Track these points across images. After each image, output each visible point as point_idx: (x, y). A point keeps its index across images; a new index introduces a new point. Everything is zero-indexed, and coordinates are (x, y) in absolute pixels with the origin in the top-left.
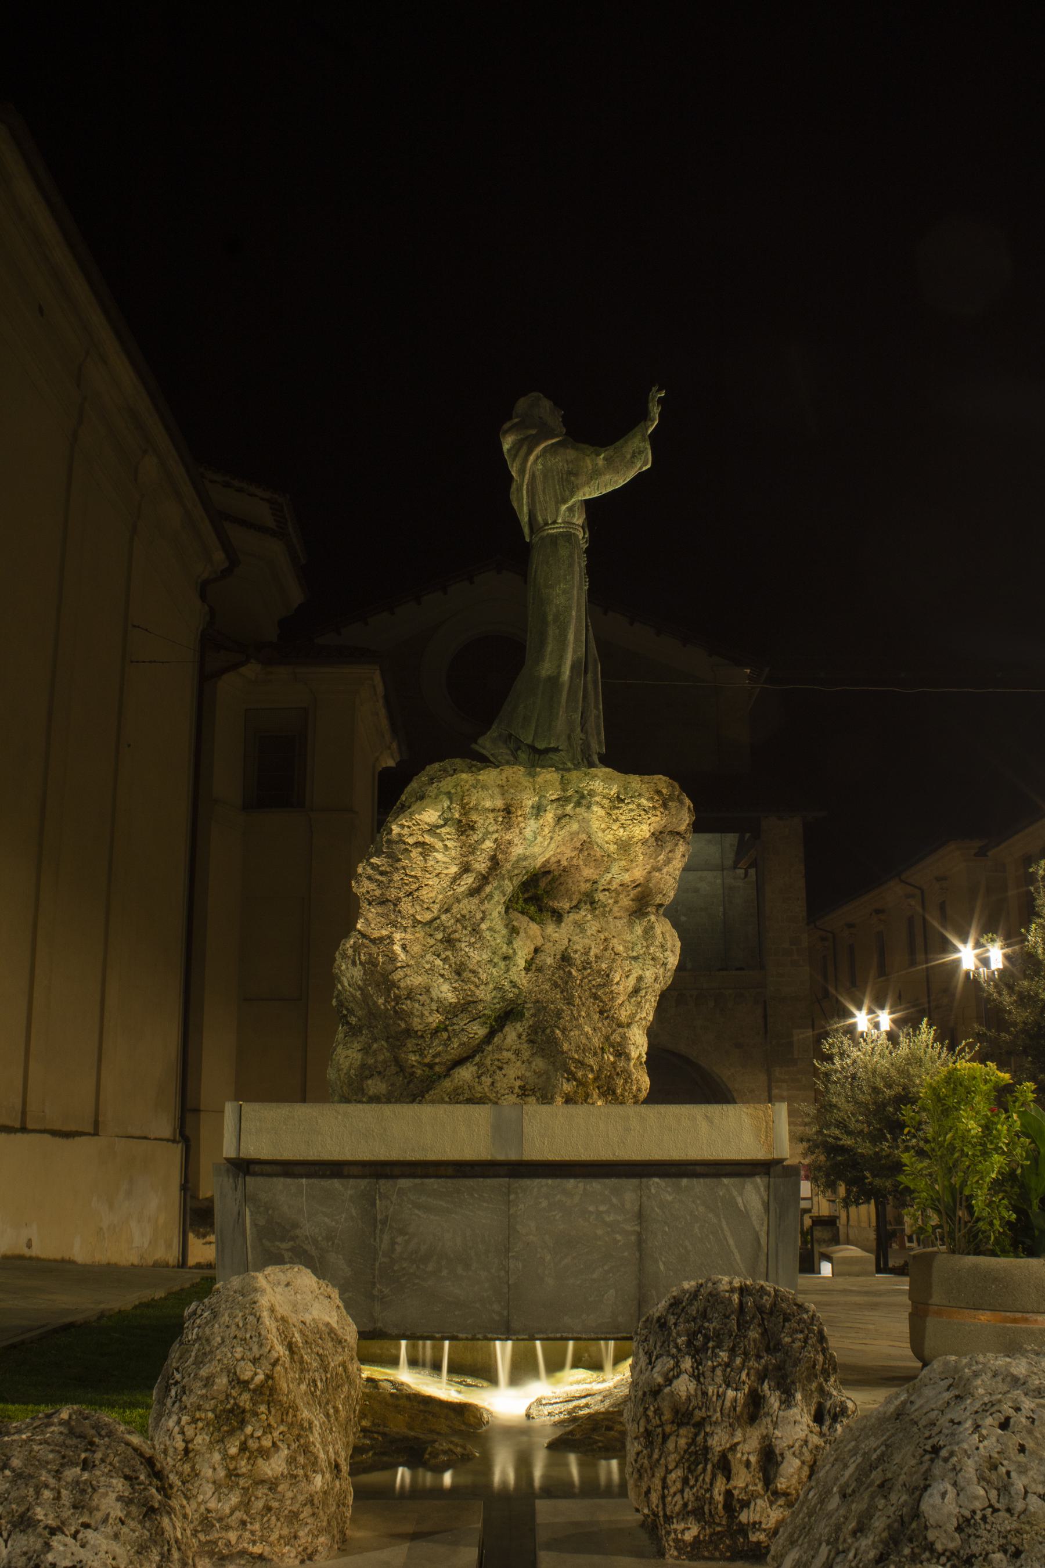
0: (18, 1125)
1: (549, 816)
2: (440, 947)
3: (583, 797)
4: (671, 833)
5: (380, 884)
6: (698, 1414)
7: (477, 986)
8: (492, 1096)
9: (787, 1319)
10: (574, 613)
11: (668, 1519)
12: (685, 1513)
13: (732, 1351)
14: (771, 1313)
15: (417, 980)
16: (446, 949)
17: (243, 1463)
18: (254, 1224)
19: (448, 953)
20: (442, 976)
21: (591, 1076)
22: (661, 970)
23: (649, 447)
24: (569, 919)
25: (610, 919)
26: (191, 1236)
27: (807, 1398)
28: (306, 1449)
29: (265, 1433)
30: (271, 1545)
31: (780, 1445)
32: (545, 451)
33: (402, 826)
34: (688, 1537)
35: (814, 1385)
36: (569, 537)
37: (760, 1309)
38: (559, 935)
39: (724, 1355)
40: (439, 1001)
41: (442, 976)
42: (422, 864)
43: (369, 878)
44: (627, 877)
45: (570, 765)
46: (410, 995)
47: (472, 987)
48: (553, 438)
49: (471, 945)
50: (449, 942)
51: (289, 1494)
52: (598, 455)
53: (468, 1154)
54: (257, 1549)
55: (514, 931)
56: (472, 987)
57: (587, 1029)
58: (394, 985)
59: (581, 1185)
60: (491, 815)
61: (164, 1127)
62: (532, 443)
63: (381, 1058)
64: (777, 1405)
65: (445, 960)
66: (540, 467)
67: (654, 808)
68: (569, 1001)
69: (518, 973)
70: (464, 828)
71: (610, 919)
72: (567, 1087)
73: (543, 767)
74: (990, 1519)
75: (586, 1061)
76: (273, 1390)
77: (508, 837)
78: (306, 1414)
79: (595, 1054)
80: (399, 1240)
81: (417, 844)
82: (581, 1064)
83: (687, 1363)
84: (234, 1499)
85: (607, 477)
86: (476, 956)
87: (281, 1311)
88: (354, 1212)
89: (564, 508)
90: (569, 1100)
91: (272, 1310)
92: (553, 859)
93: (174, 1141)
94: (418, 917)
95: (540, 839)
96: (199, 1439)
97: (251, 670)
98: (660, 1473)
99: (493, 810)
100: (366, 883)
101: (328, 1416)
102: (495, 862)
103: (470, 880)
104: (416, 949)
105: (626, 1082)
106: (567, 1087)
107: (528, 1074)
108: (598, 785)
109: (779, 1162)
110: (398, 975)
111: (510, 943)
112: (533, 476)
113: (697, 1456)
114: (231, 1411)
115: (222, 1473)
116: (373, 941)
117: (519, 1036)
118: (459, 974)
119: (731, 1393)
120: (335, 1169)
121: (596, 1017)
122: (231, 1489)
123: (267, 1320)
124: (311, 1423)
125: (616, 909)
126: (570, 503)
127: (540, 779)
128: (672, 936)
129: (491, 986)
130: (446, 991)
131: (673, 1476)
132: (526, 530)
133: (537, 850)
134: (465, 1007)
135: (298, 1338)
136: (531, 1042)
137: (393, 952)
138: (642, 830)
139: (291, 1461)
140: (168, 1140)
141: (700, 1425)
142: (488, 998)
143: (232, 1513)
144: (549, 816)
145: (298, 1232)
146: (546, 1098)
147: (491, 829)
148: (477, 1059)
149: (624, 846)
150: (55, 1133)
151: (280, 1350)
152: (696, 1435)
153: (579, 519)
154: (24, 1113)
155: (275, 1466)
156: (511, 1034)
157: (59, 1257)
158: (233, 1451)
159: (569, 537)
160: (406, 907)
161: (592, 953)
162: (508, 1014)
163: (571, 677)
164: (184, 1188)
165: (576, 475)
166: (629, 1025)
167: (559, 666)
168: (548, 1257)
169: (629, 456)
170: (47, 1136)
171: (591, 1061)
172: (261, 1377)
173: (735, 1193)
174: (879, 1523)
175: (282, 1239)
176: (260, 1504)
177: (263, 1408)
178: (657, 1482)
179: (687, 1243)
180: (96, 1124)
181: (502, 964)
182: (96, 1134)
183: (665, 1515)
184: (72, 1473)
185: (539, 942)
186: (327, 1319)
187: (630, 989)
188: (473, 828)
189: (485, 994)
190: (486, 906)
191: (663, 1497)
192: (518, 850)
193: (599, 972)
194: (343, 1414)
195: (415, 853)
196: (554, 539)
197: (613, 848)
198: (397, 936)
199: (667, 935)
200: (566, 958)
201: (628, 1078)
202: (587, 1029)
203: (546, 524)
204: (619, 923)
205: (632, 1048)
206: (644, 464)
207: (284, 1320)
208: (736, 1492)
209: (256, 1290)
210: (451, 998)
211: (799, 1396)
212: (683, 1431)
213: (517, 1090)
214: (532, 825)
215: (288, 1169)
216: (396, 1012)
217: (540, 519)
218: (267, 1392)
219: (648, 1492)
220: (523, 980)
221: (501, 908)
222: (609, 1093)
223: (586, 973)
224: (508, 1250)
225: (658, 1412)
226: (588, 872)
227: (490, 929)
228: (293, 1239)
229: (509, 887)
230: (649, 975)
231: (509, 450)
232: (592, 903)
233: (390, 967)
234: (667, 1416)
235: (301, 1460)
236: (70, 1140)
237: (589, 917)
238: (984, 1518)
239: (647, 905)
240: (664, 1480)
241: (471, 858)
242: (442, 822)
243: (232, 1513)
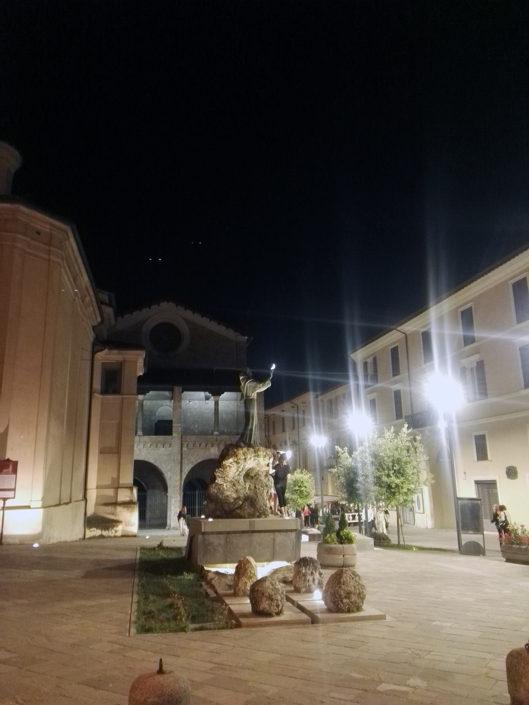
1: (252, 459)
15: (228, 493)
36: (254, 399)
46: (227, 496)
50: (234, 485)
53: (246, 529)
55: (245, 482)
68: (257, 497)
70: (237, 463)
97: (106, 351)
102: (243, 469)
104: (228, 487)
106: (258, 514)
110: (225, 492)
120: (220, 533)
130: (234, 495)
134: (238, 498)
144: (252, 459)
153: (256, 395)
160: (226, 478)
189: (242, 496)
192: (246, 467)
195: (228, 468)
196: (252, 399)
198: (225, 484)
206: (270, 385)
214: (249, 462)
215: (212, 533)
226: (258, 469)
229: (244, 473)
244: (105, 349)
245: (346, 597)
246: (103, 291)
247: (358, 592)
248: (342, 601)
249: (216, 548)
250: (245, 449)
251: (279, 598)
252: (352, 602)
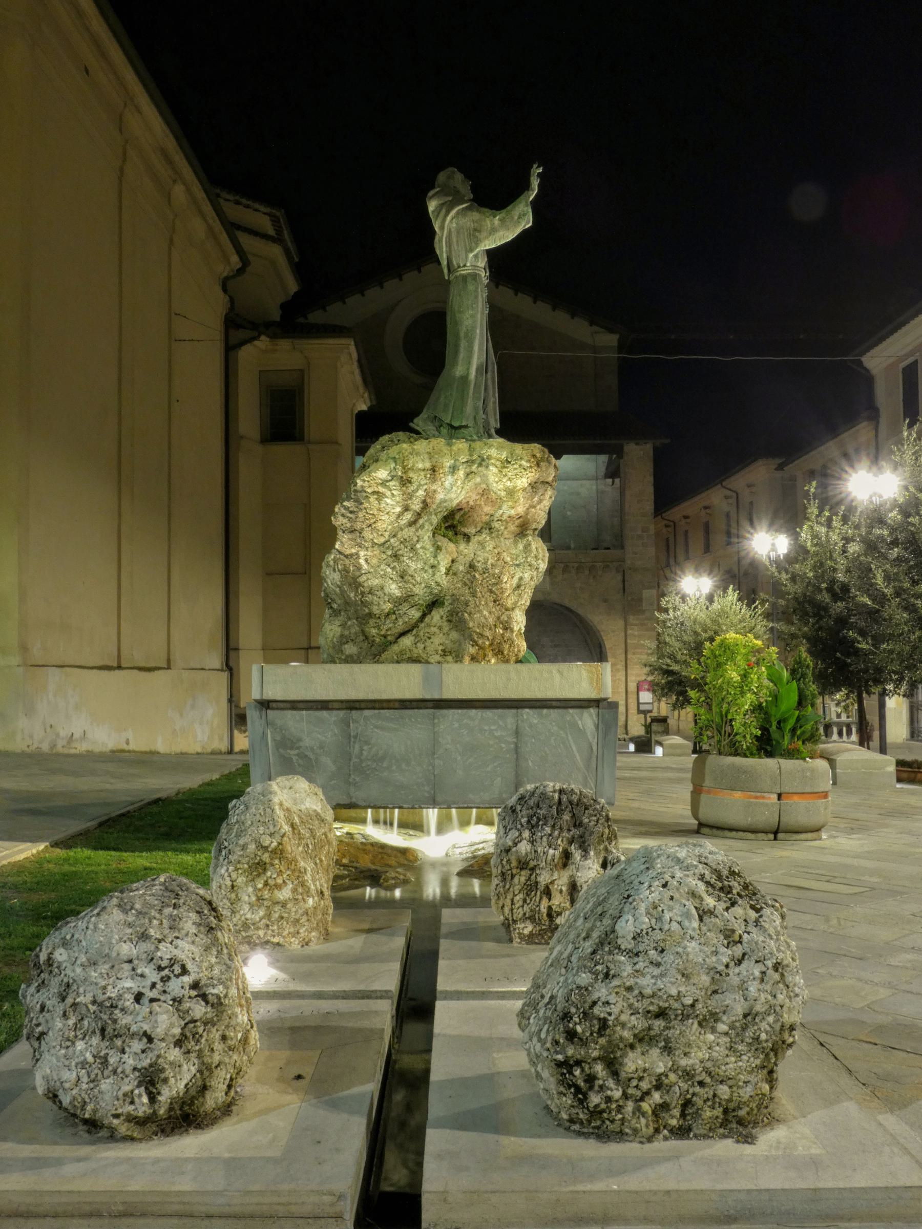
0: (115, 665)
1: (461, 473)
2: (390, 560)
3: (483, 460)
4: (543, 482)
5: (350, 519)
6: (532, 864)
7: (414, 586)
8: (424, 656)
9: (586, 809)
10: (478, 331)
11: (515, 922)
12: (525, 918)
13: (553, 826)
14: (577, 805)
15: (375, 582)
16: (393, 561)
17: (266, 892)
18: (274, 740)
19: (395, 564)
20: (392, 579)
21: (487, 643)
22: (535, 573)
23: (530, 210)
24: (475, 540)
25: (502, 539)
26: (236, 732)
27: (597, 854)
28: (303, 884)
29: (278, 875)
30: (284, 937)
31: (580, 881)
32: (458, 213)
33: (364, 481)
34: (526, 932)
35: (602, 847)
36: (475, 276)
37: (571, 803)
38: (467, 550)
39: (548, 830)
40: (390, 595)
41: (392, 579)
42: (377, 506)
43: (343, 515)
44: (513, 512)
45: (475, 437)
47: (411, 586)
48: (463, 204)
49: (410, 558)
50: (396, 556)
51: (294, 909)
52: (495, 217)
53: (408, 695)
54: (276, 940)
55: (438, 548)
56: (411, 586)
57: (485, 613)
58: (360, 585)
59: (480, 714)
60: (422, 473)
61: (215, 660)
62: (450, 206)
63: (353, 631)
64: (579, 858)
65: (393, 569)
66: (454, 225)
67: (531, 467)
68: (474, 595)
69: (441, 576)
70: (405, 482)
71: (502, 539)
72: (473, 650)
73: (457, 438)
74: (650, 934)
75: (484, 633)
76: (282, 851)
77: (434, 487)
78: (302, 864)
79: (490, 629)
80: (365, 748)
81: (374, 493)
82: (481, 635)
83: (526, 834)
84: (261, 913)
85: (501, 233)
86: (413, 566)
87: (286, 805)
88: (336, 731)
89: (471, 255)
90: (473, 659)
91: (281, 805)
92: (464, 501)
93: (222, 670)
94: (375, 541)
95: (455, 488)
96: (239, 880)
98: (510, 896)
99: (424, 470)
100: (341, 518)
101: (316, 864)
102: (425, 504)
103: (409, 516)
104: (374, 561)
105: (510, 646)
107: (447, 642)
108: (493, 452)
109: (605, 699)
110: (364, 578)
111: (435, 557)
112: (450, 232)
113: (531, 887)
114: (258, 864)
115: (254, 899)
116: (346, 556)
117: (442, 617)
118: (402, 577)
119: (551, 851)
120: (324, 705)
121: (491, 604)
122: (259, 907)
123: (278, 811)
124: (305, 869)
125: (506, 533)
126: (475, 252)
127: (455, 448)
128: (543, 550)
129: (423, 585)
130: (394, 589)
131: (518, 898)
132: (446, 271)
133: (453, 495)
134: (406, 598)
135: (297, 820)
136: (449, 621)
137: (359, 564)
138: (523, 482)
139: (294, 891)
140: (218, 670)
141: (533, 869)
142: (421, 593)
143: (261, 920)
144: (461, 473)
145: (301, 744)
146: (458, 659)
147: (422, 483)
148: (414, 632)
149: (511, 493)
150: (141, 669)
151: (286, 828)
152: (531, 875)
153: (482, 263)
154: (119, 656)
155: (285, 894)
156: (437, 616)
157: (147, 749)
158: (260, 886)
159: (475, 276)
160: (367, 534)
161: (489, 563)
162: (434, 604)
163: (476, 377)
164: (230, 701)
165: (479, 231)
166: (513, 609)
167: (468, 369)
168: (459, 758)
169: (516, 218)
170: (136, 671)
171: (488, 633)
172: (275, 844)
173: (577, 718)
174: (595, 935)
175: (292, 748)
176: (277, 915)
177: (277, 861)
178: (508, 902)
179: (546, 749)
180: (169, 661)
181: (430, 571)
182: (169, 668)
183: (513, 920)
184: (168, 911)
185: (455, 555)
186: (315, 807)
187: (514, 585)
188: (410, 482)
189: (419, 590)
190: (420, 532)
191: (512, 910)
192: (440, 496)
193: (493, 575)
194: (325, 863)
195: (372, 499)
196: (465, 278)
197: (503, 494)
198: (362, 553)
199: (540, 551)
200: (472, 566)
201: (512, 643)
202: (485, 613)
203: (459, 267)
204: (507, 542)
205: (515, 624)
206: (527, 223)
207: (288, 810)
208: (554, 907)
209: (271, 793)
210: (397, 593)
211: (592, 853)
212: (523, 873)
213: (440, 652)
215: (294, 705)
216: (362, 602)
217: (455, 263)
218: (279, 852)
219: (503, 907)
220: (444, 581)
221: (430, 534)
222: (499, 653)
223: (485, 576)
224: (434, 754)
225: (509, 861)
226: (487, 509)
227: (423, 548)
228: (298, 748)
229: (435, 520)
230: (527, 576)
231: (433, 212)
232: (490, 529)
233: (358, 574)
234: (514, 864)
235: (300, 890)
236: (152, 673)
237: (488, 538)
238: (647, 933)
239: (526, 529)
240: (512, 900)
241: (409, 502)
242: (390, 478)
243: (261, 920)
244: (259, 336)
245: (644, 1039)
246: (257, 206)
247: (739, 1009)
248: (613, 1065)
249: (312, 757)
250: (439, 443)
251: (165, 1022)
252: (688, 1075)
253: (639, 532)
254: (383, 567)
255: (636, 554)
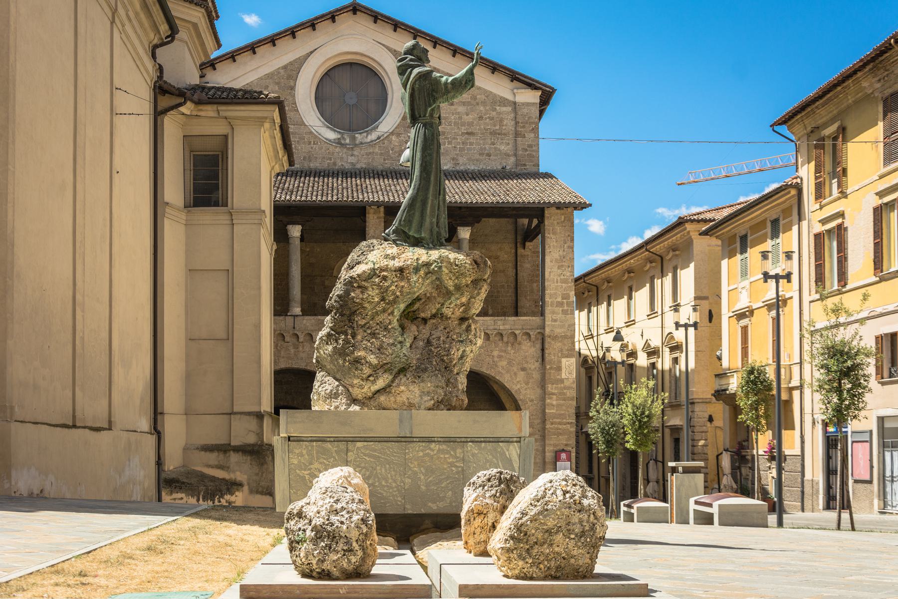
0: (71, 424)
26: (163, 494)
38: (425, 331)
45: (431, 245)
49: (384, 336)
61: (144, 424)
93: (151, 434)
111: (402, 335)
145: (312, 466)
170: (87, 430)
180: (110, 422)
181: (399, 346)
182: (110, 429)
253: (559, 299)
254: (365, 342)
255: (555, 321)
